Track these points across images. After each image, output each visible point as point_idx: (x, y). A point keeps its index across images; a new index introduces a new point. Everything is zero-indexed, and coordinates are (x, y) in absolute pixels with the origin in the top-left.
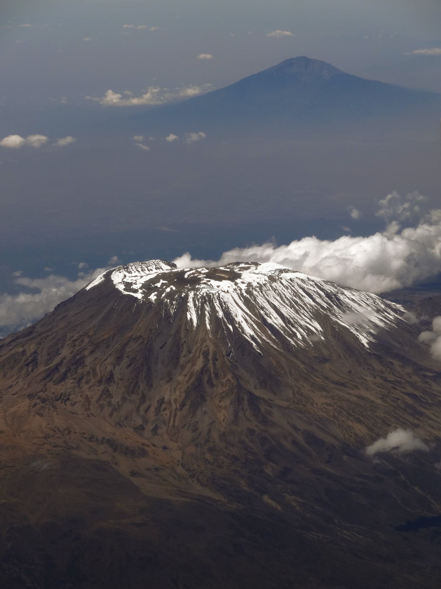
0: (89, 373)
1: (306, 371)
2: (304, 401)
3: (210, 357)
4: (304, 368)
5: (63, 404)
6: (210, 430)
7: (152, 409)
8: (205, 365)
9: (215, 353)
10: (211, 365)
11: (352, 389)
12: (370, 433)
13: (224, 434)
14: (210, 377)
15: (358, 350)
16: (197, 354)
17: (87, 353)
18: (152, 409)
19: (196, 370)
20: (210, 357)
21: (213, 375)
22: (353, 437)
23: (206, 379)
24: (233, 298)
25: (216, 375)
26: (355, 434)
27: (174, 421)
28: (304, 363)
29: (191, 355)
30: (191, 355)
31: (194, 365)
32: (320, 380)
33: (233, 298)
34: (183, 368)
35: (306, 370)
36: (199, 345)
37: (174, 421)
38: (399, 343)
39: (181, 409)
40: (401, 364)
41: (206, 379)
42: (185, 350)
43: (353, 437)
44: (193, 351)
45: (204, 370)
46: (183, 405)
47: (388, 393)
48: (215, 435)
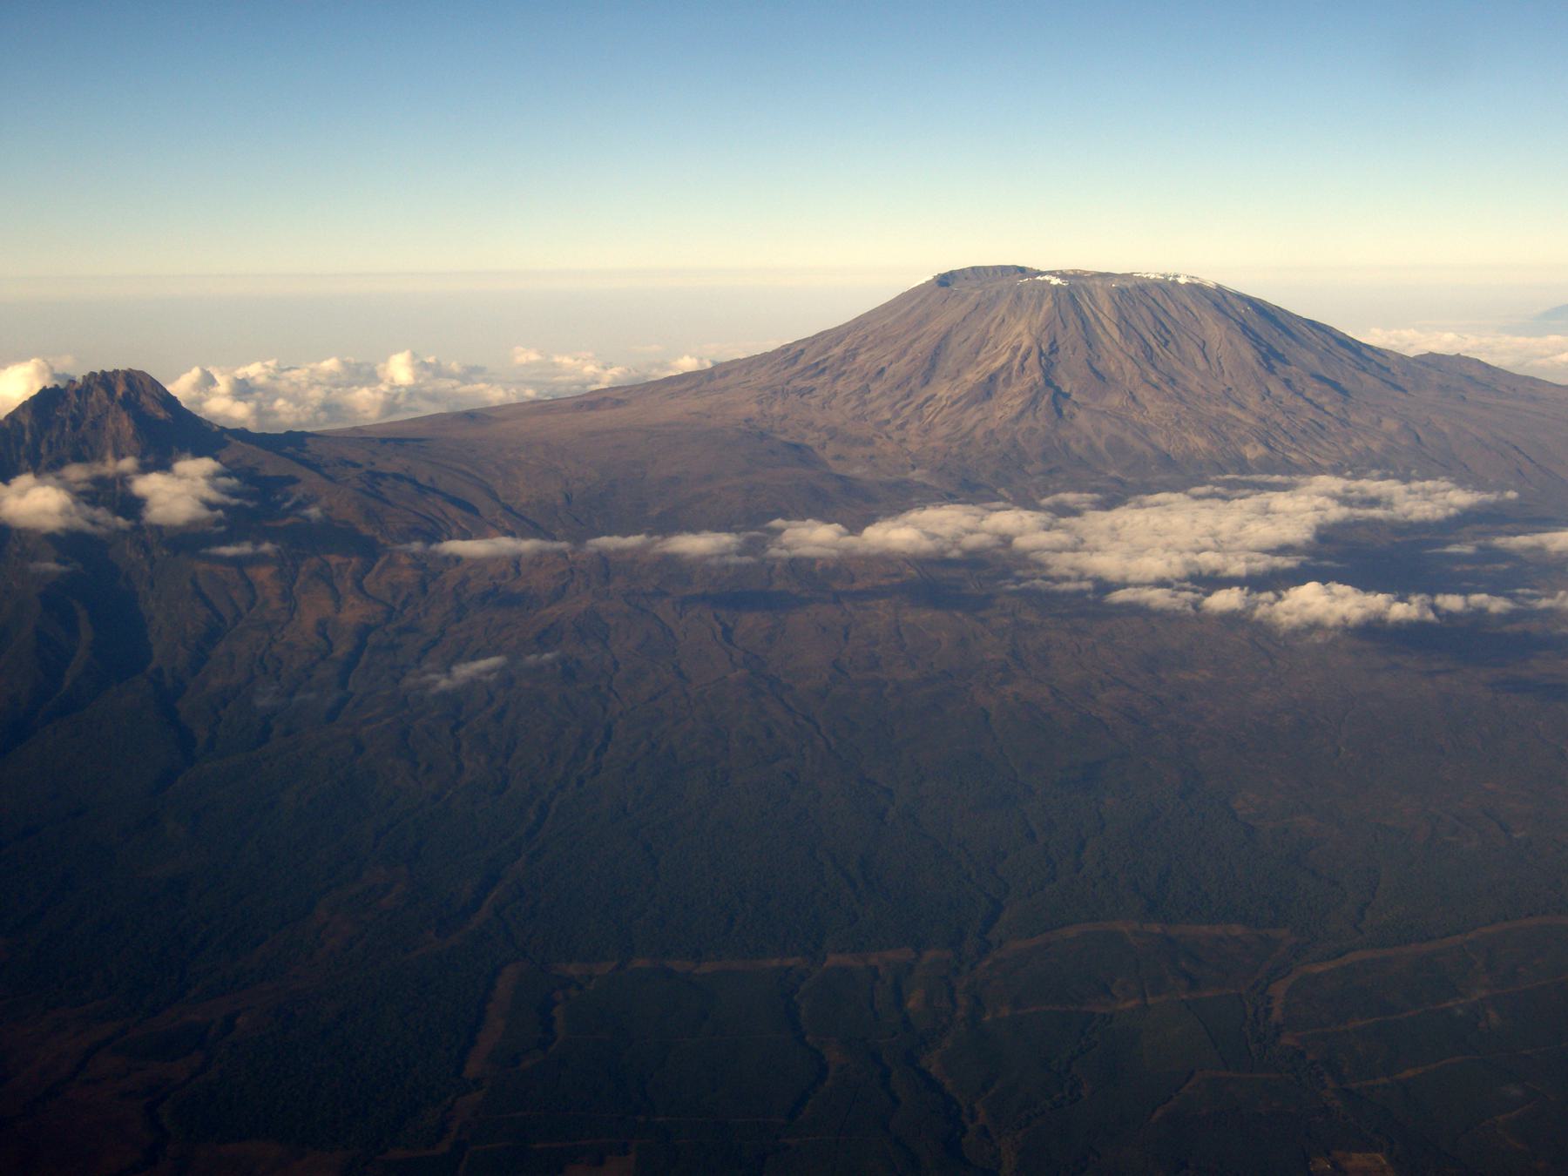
0: (852, 371)
3: (1020, 353)
5: (798, 397)
6: (975, 426)
7: (914, 405)
8: (1008, 362)
13: (992, 432)
14: (1010, 374)
16: (1003, 351)
17: (863, 350)
18: (914, 405)
20: (1020, 353)
21: (1014, 373)
23: (1003, 376)
27: (935, 417)
29: (997, 350)
30: (997, 350)
31: (994, 361)
34: (978, 365)
36: (1010, 339)
37: (935, 417)
39: (950, 407)
41: (1003, 376)
42: (990, 345)
44: (1000, 347)
45: (1006, 367)
46: (954, 403)
48: (979, 432)
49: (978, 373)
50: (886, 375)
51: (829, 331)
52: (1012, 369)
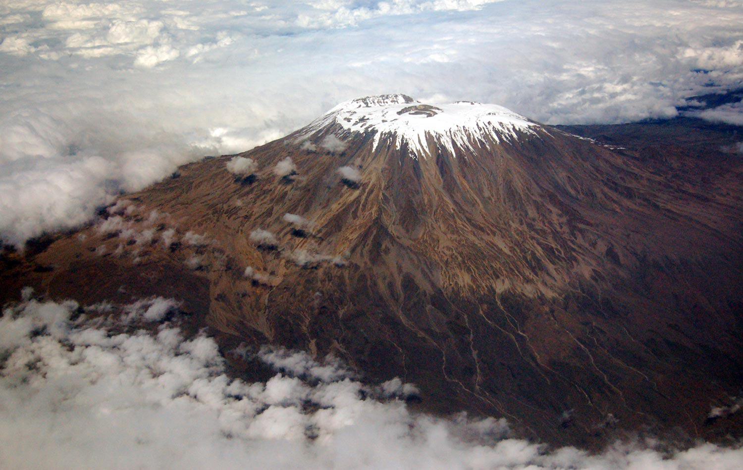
1: (452, 211)
2: (429, 242)
3: (367, 190)
4: (452, 208)
9: (374, 185)
10: (364, 197)
11: (488, 234)
12: (472, 284)
14: (357, 208)
15: (520, 195)
19: (349, 200)
20: (367, 190)
21: (361, 206)
22: (452, 286)
24: (419, 138)
25: (364, 206)
26: (456, 283)
28: (456, 203)
32: (460, 222)
33: (419, 138)
35: (454, 210)
38: (576, 190)
40: (560, 212)
43: (452, 286)
47: (523, 242)
49: (339, 204)
50: (286, 199)
51: (274, 141)
52: (360, 203)
